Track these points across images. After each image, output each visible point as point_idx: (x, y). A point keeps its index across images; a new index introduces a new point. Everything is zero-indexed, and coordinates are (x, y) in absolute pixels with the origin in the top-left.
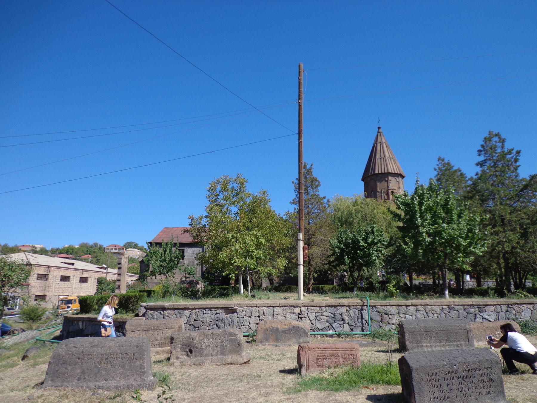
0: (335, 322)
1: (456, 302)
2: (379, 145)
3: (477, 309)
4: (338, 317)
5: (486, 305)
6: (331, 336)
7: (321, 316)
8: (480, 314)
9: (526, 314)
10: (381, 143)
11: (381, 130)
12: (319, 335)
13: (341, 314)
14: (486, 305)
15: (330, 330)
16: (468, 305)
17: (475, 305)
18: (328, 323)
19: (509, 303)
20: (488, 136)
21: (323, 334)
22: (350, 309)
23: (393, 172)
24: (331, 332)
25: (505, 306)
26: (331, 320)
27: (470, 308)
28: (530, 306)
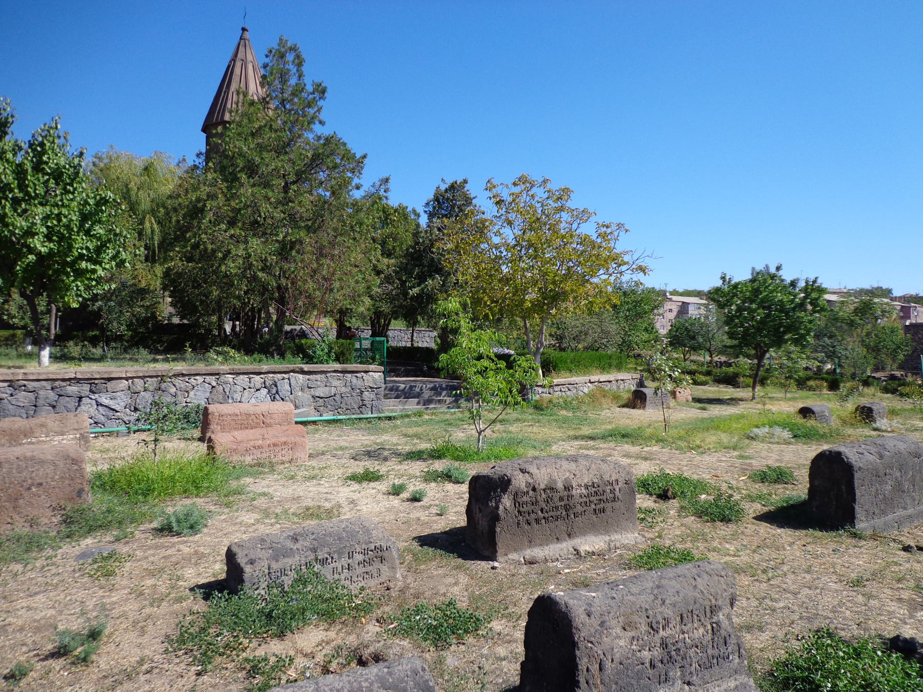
1: (33, 374)
2: (238, 64)
3: (86, 387)
5: (110, 379)
8: (93, 397)
9: (198, 393)
10: (244, 62)
11: (247, 35)
14: (110, 379)
16: (64, 380)
17: (80, 379)
19: (164, 374)
20: (277, 47)
25: (155, 379)
27: (70, 385)
28: (212, 380)
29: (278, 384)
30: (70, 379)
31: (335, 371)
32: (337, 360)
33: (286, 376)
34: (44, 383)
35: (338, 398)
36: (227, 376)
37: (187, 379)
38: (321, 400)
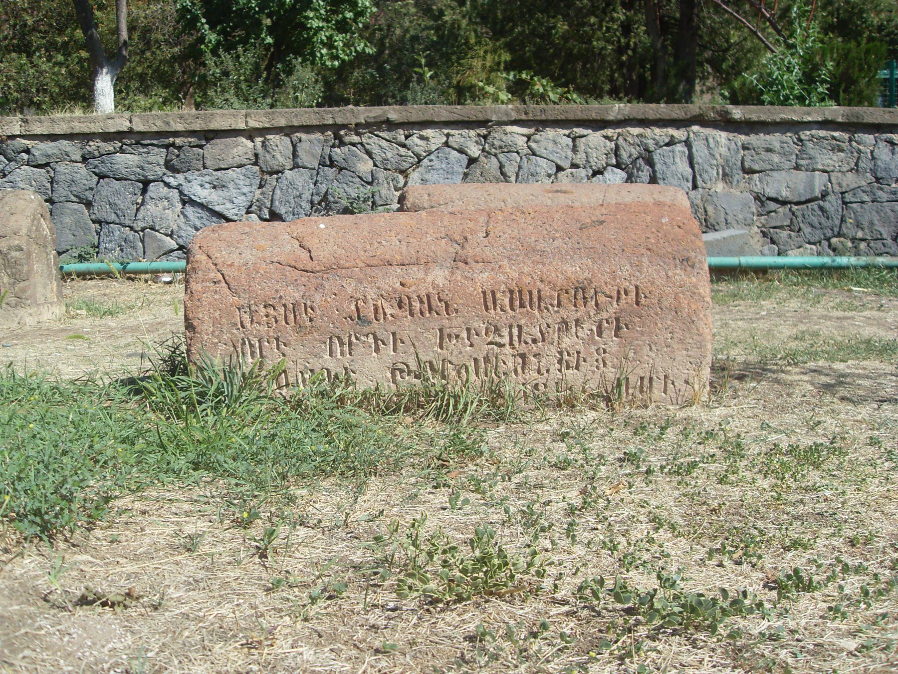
9: (431, 176)
16: (107, 137)
17: (143, 134)
25: (318, 136)
27: (122, 151)
28: (469, 139)
29: (656, 158)
30: (119, 135)
31: (826, 124)
32: (833, 96)
33: (679, 134)
34: (64, 144)
35: (832, 204)
36: (509, 128)
37: (400, 135)
38: (781, 210)
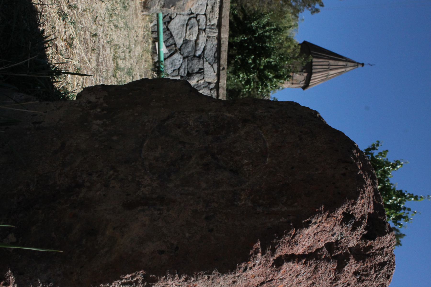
0: (184, 58)
2: (344, 63)
4: (196, 65)
6: (155, 52)
7: (196, 29)
10: (345, 67)
11: (360, 66)
12: (155, 22)
13: (201, 71)
15: (167, 47)
18: (181, 42)
21: (158, 31)
22: (211, 89)
23: (312, 78)
24: (164, 50)
26: (190, 49)
